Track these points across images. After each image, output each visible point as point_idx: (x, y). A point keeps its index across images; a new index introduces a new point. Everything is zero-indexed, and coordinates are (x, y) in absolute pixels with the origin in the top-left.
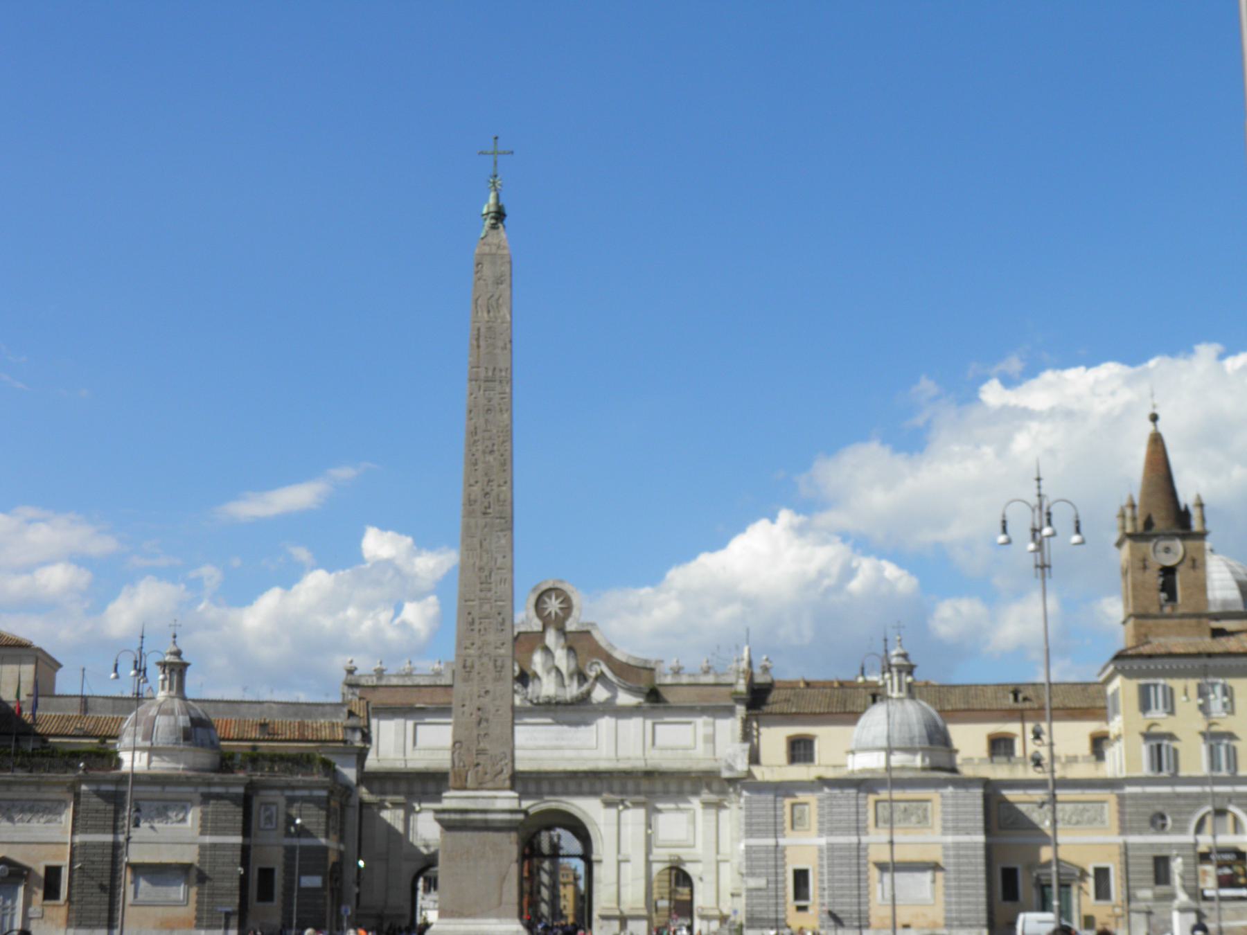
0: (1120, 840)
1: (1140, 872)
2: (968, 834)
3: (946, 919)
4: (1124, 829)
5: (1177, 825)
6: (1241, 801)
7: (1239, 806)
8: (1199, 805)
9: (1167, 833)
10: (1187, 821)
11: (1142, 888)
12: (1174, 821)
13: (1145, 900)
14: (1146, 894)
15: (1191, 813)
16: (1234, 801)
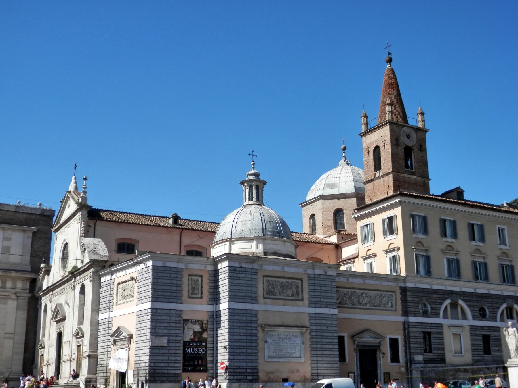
0: (402, 319)
1: (416, 343)
2: (327, 307)
3: (312, 375)
4: (406, 313)
5: (434, 311)
6: (466, 298)
7: (464, 301)
8: (445, 299)
9: (429, 317)
10: (439, 309)
11: (418, 354)
12: (432, 309)
13: (419, 362)
14: (419, 358)
15: (441, 304)
16: (462, 298)
